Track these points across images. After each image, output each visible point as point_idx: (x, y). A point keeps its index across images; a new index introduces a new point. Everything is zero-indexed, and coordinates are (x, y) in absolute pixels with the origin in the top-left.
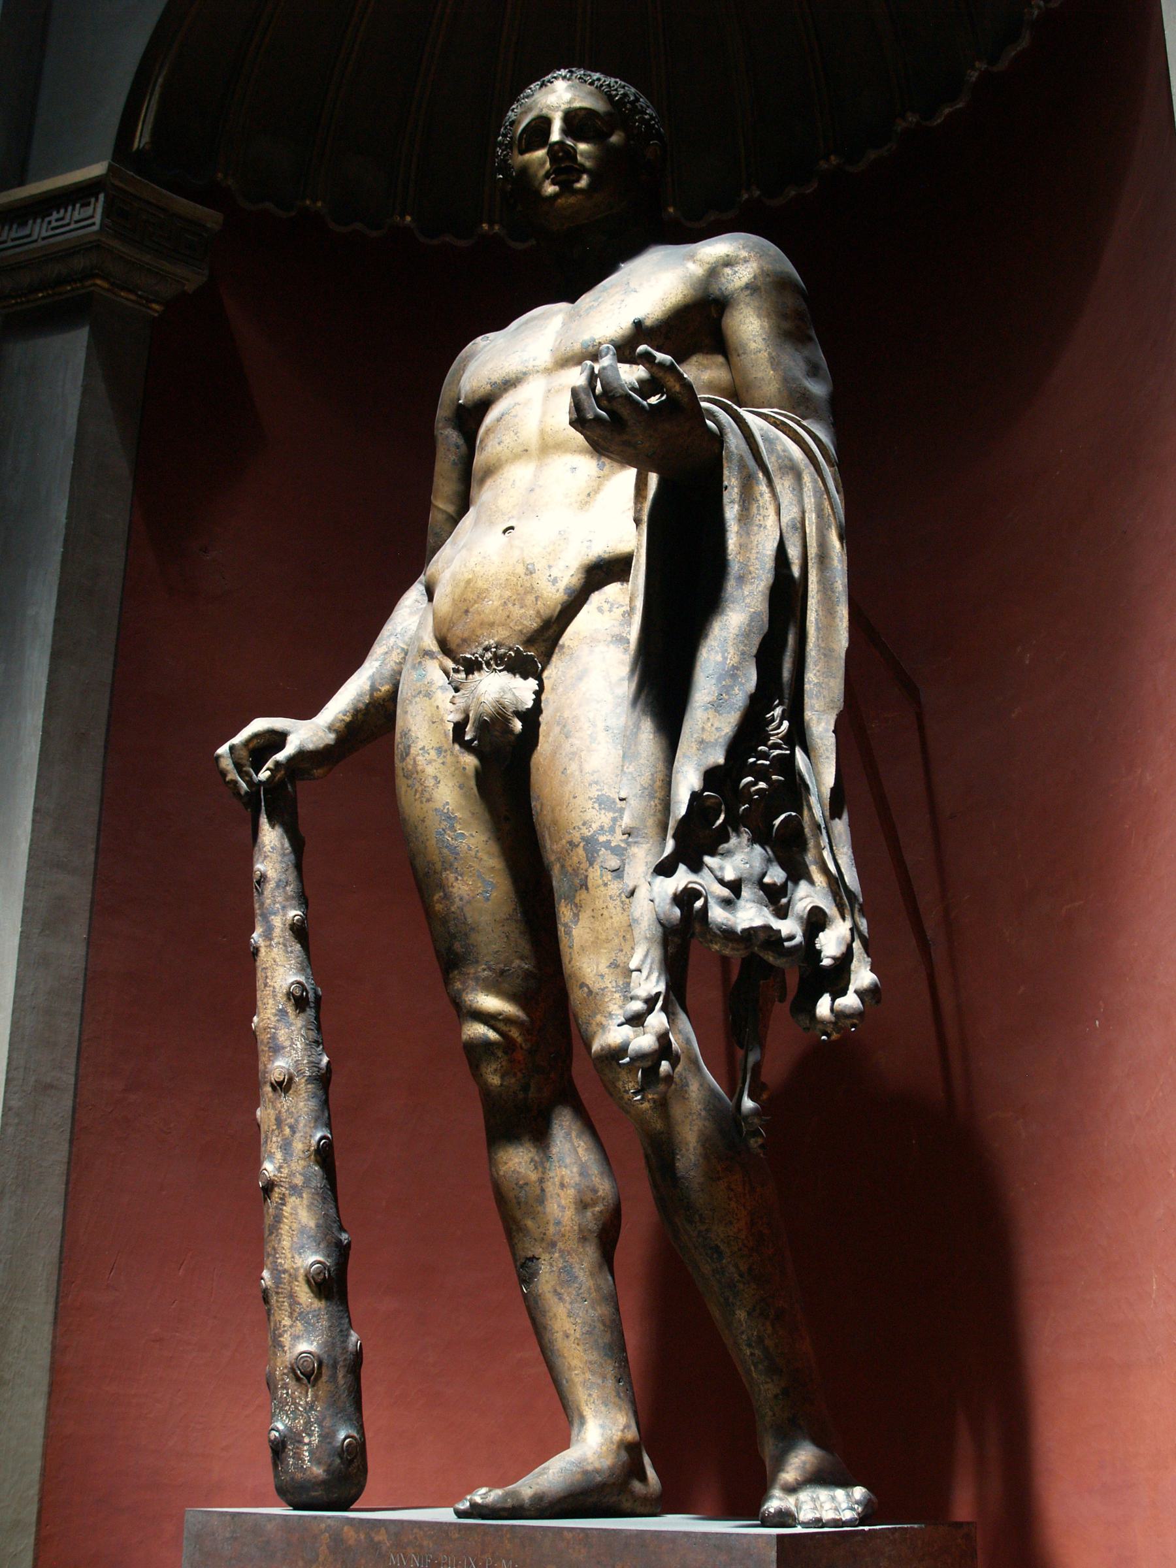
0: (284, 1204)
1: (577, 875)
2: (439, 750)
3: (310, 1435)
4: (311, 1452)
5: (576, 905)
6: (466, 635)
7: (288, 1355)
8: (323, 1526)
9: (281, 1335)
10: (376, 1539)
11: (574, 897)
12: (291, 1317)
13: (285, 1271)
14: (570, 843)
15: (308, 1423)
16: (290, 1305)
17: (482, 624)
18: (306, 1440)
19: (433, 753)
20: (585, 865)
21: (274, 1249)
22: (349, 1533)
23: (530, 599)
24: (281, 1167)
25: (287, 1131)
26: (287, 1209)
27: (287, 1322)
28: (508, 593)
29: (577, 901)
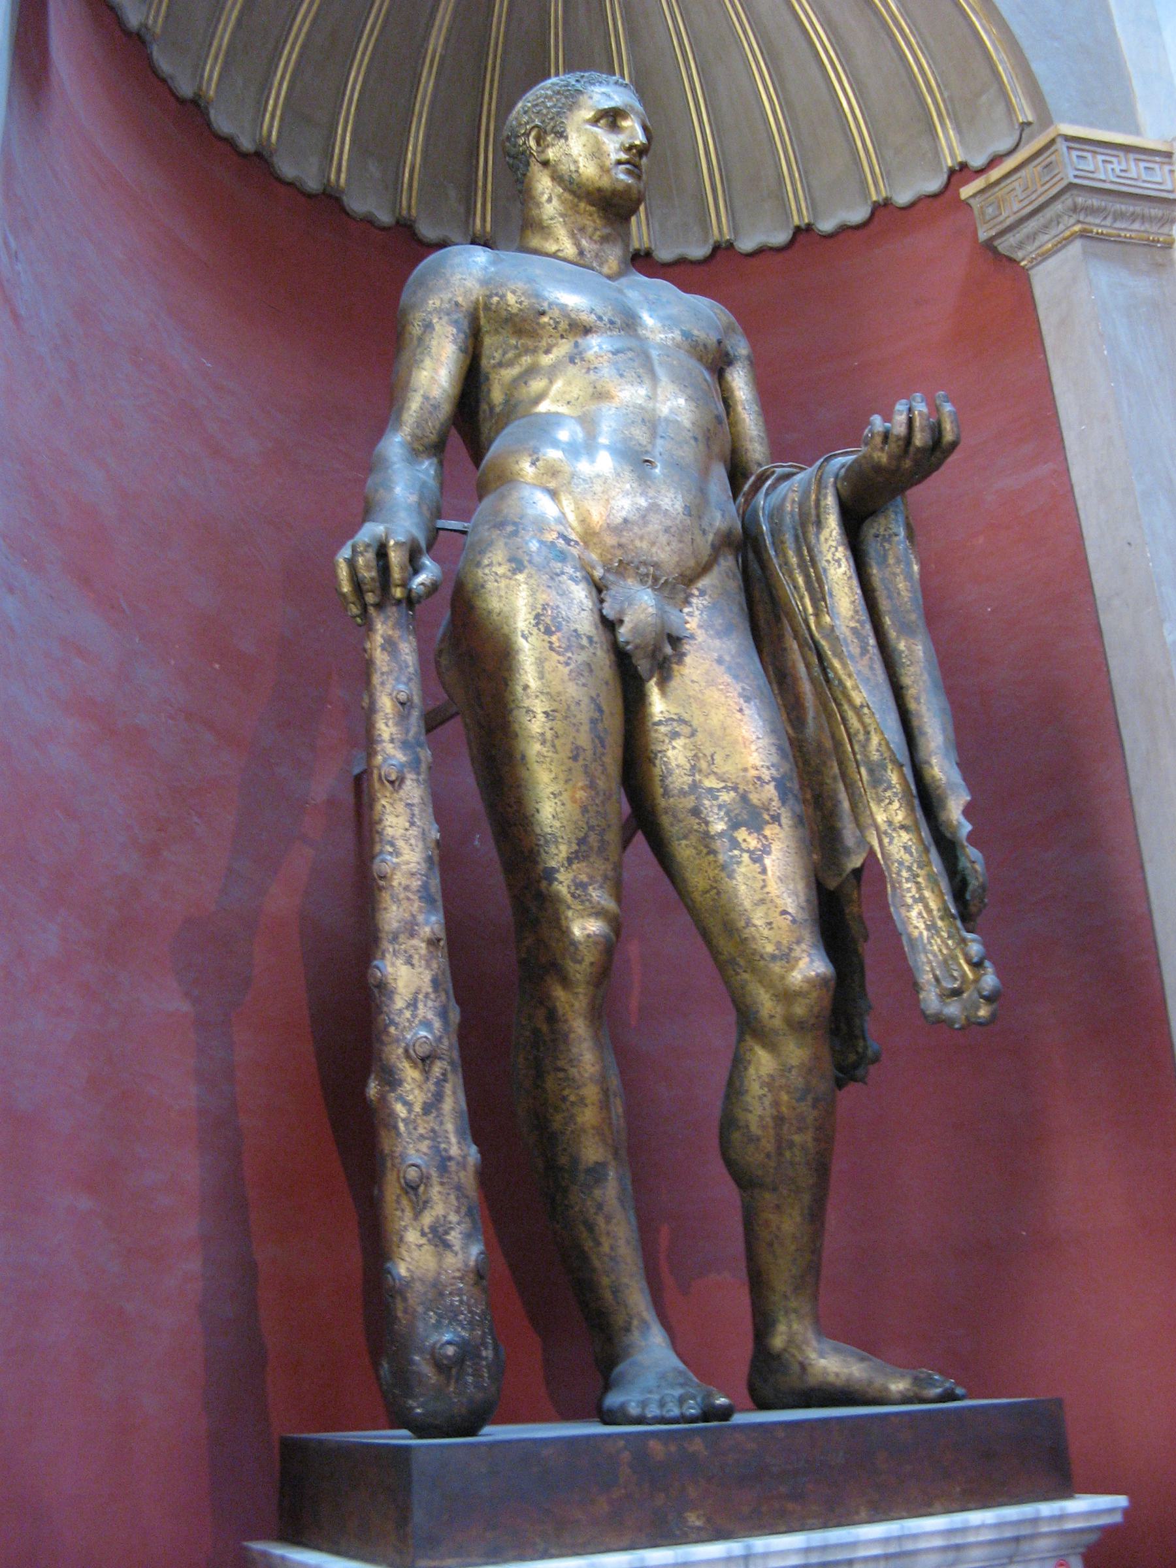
0: (445, 1081)
1: (768, 810)
2: (590, 639)
3: (486, 1348)
4: (488, 1367)
5: (765, 837)
6: (623, 540)
7: (460, 1256)
8: (622, 1443)
9: (447, 1233)
10: (691, 1449)
11: (762, 829)
12: (457, 1212)
13: (450, 1158)
14: (759, 778)
15: (483, 1337)
16: (458, 1198)
17: (641, 538)
18: (484, 1354)
19: (585, 642)
20: (776, 803)
21: (433, 1131)
22: (655, 1446)
23: (688, 538)
24: (439, 1040)
25: (443, 997)
26: (448, 1088)
27: (453, 1218)
28: (669, 523)
29: (767, 832)
